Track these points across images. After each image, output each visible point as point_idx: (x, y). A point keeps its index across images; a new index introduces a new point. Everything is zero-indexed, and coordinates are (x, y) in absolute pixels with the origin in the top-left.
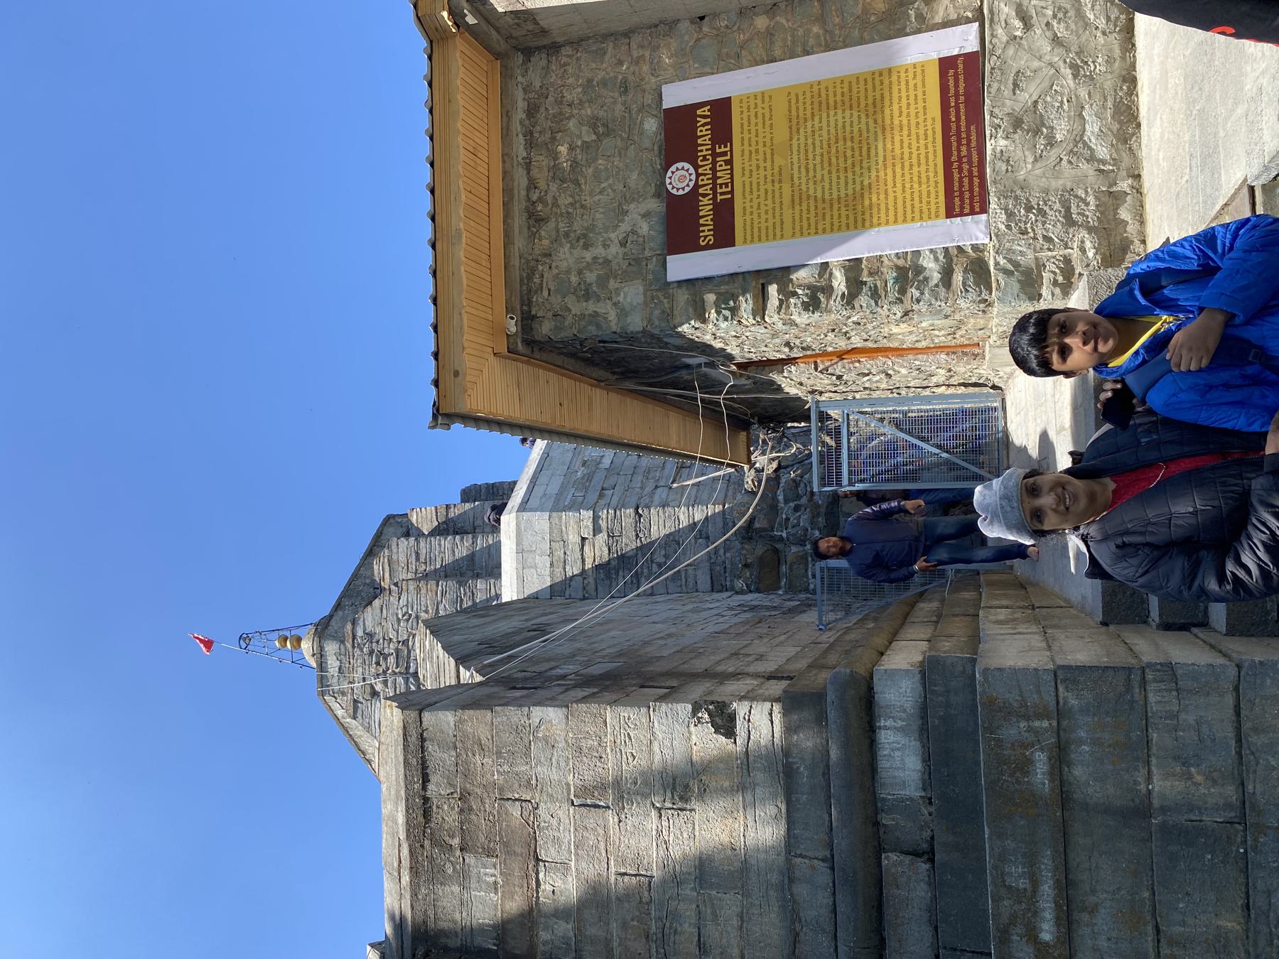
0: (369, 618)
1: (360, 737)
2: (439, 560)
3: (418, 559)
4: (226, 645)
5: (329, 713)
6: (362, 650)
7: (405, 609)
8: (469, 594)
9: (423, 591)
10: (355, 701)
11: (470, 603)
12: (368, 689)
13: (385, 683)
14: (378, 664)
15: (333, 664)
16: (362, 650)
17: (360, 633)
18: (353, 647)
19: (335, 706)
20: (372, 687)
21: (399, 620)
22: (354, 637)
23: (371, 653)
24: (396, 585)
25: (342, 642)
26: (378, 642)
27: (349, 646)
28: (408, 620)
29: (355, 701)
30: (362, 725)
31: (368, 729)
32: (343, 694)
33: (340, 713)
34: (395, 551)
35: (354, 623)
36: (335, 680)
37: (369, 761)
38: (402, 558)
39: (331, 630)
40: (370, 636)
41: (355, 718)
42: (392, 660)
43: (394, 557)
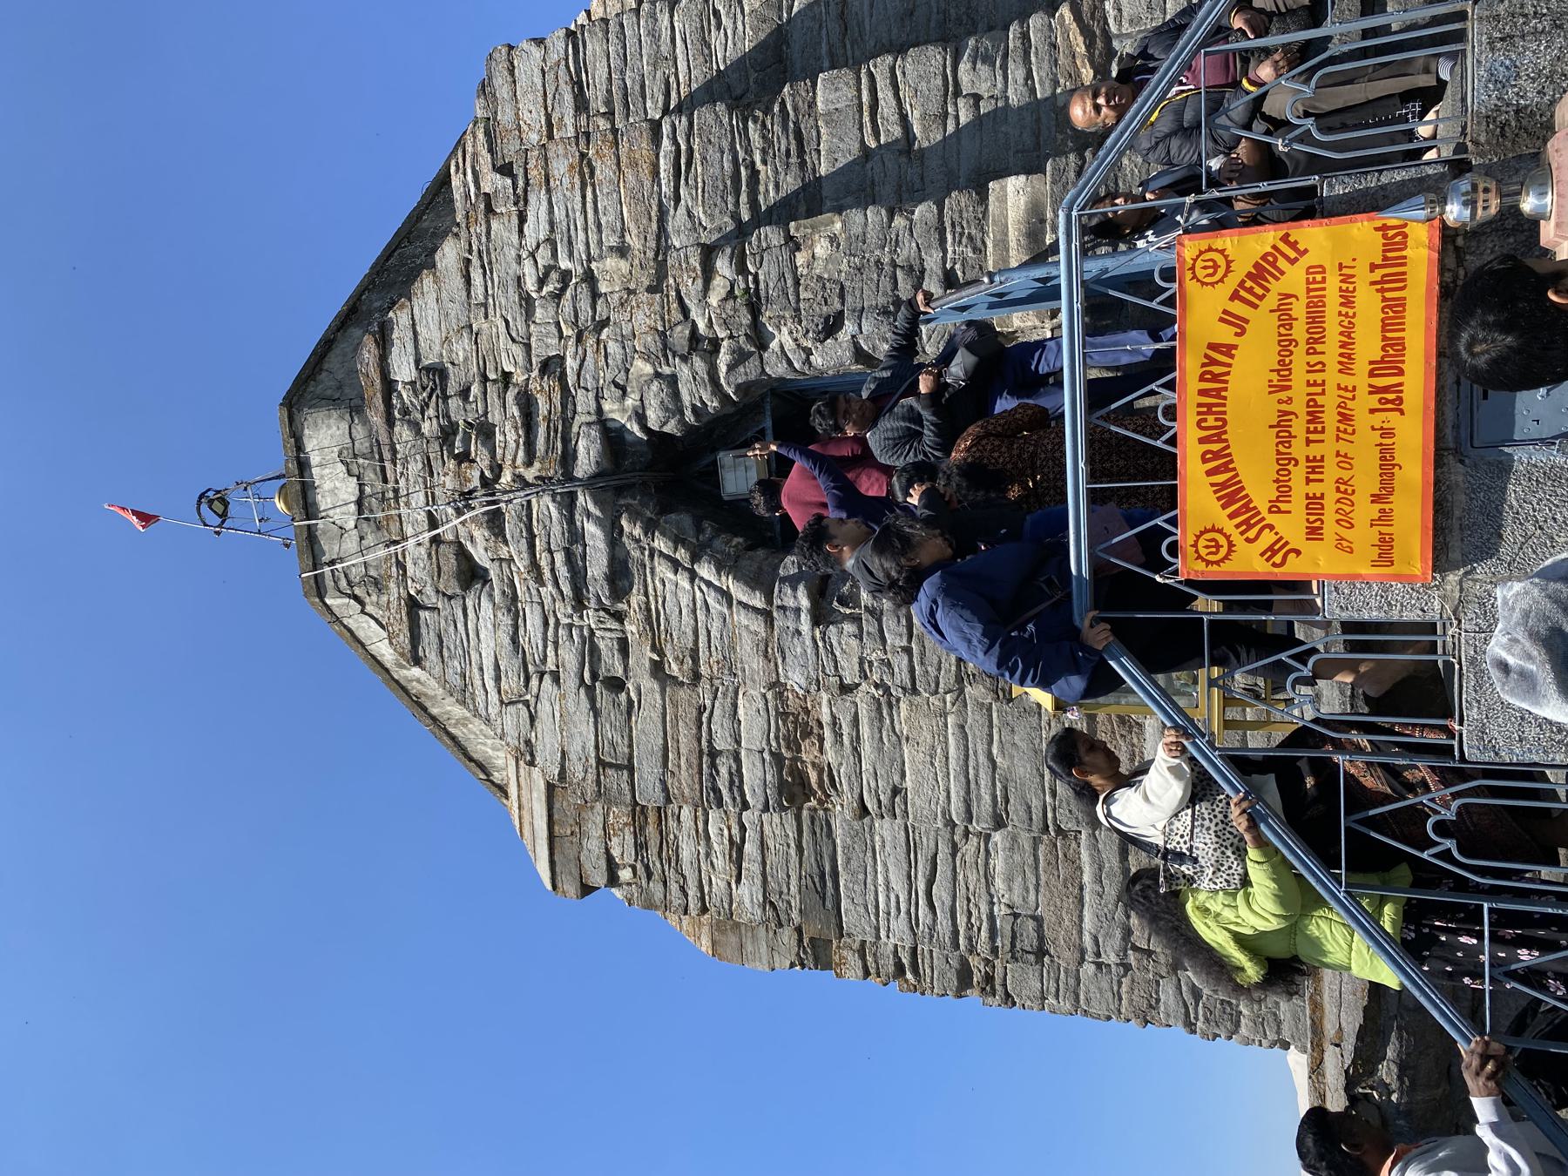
0: (428, 321)
1: (463, 722)
2: (655, 89)
3: (581, 104)
4: (181, 519)
5: (354, 653)
6: (416, 427)
7: (543, 257)
8: (783, 143)
9: (604, 170)
10: (414, 605)
11: (791, 183)
12: (450, 563)
13: (495, 522)
14: (464, 458)
15: (335, 490)
16: (416, 427)
17: (403, 370)
18: (390, 422)
19: (367, 629)
20: (463, 554)
21: (527, 304)
22: (389, 386)
23: (447, 434)
24: (505, 170)
25: (356, 409)
26: (464, 393)
27: (377, 419)
28: (557, 296)
29: (413, 606)
30: (443, 682)
31: (463, 695)
32: (378, 585)
33: (386, 653)
34: (503, 92)
35: (384, 343)
36: (351, 543)
37: (502, 790)
38: (532, 116)
39: (325, 382)
40: (435, 375)
41: (417, 661)
42: (509, 436)
43: (505, 116)
